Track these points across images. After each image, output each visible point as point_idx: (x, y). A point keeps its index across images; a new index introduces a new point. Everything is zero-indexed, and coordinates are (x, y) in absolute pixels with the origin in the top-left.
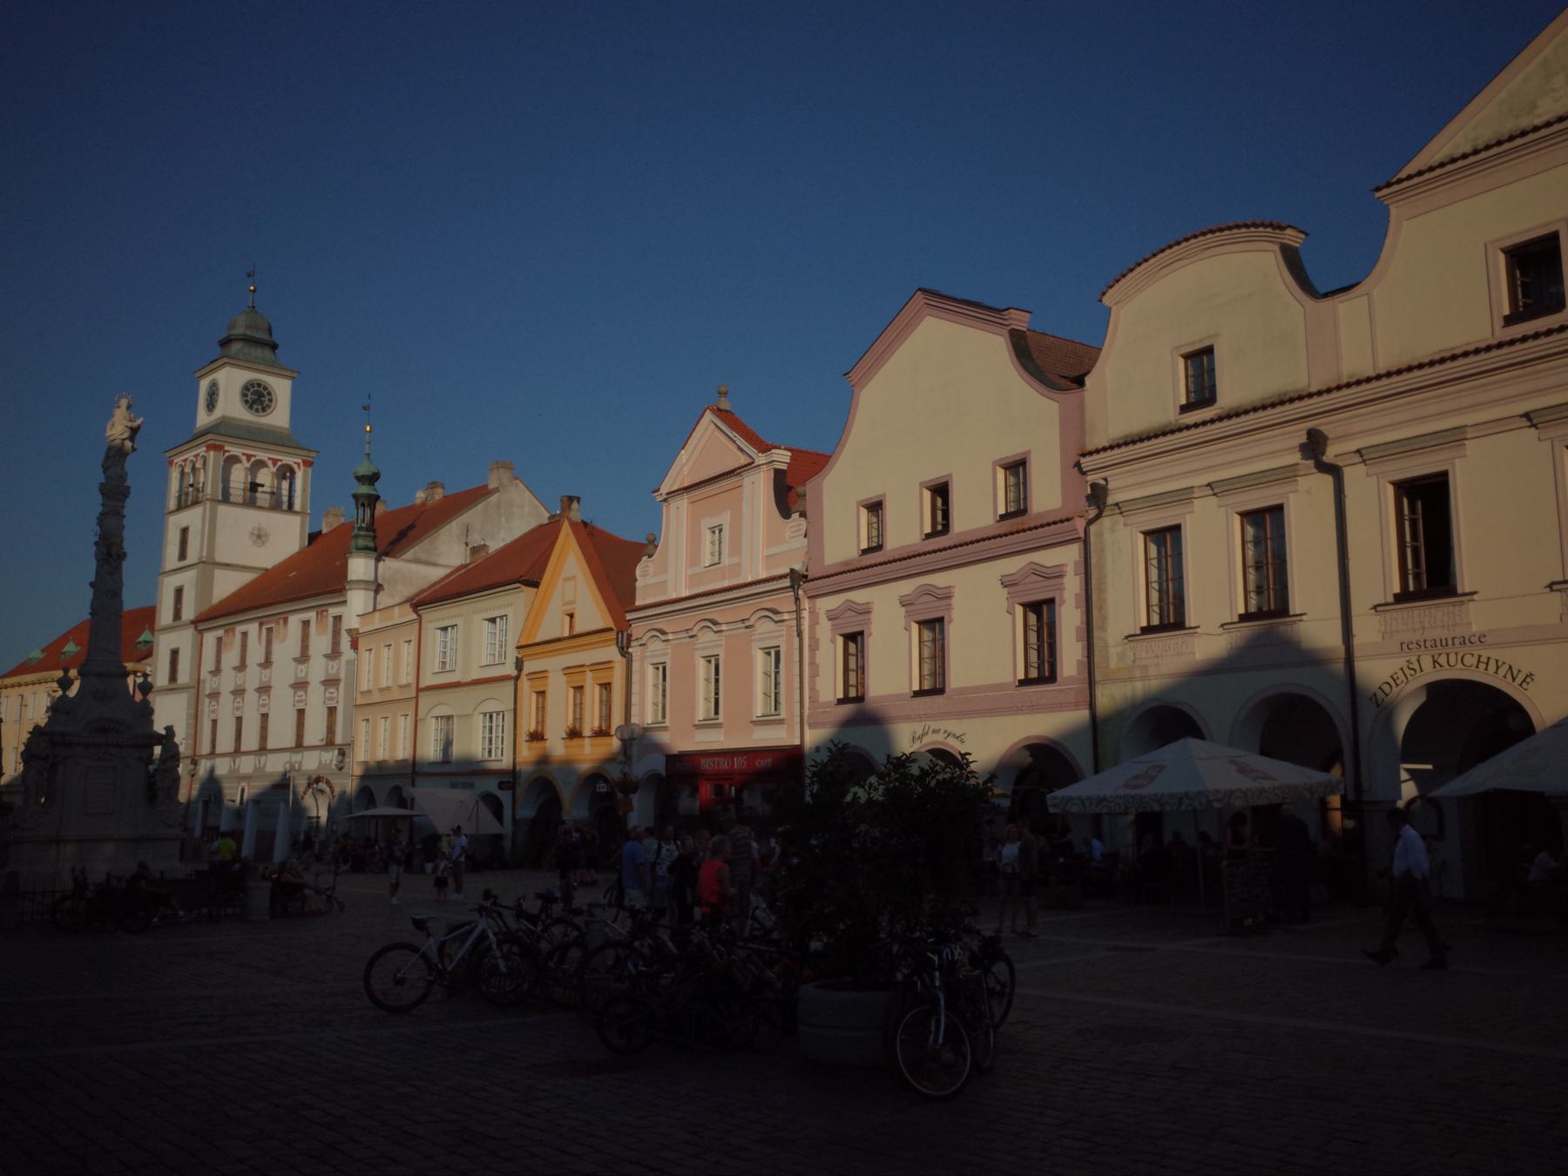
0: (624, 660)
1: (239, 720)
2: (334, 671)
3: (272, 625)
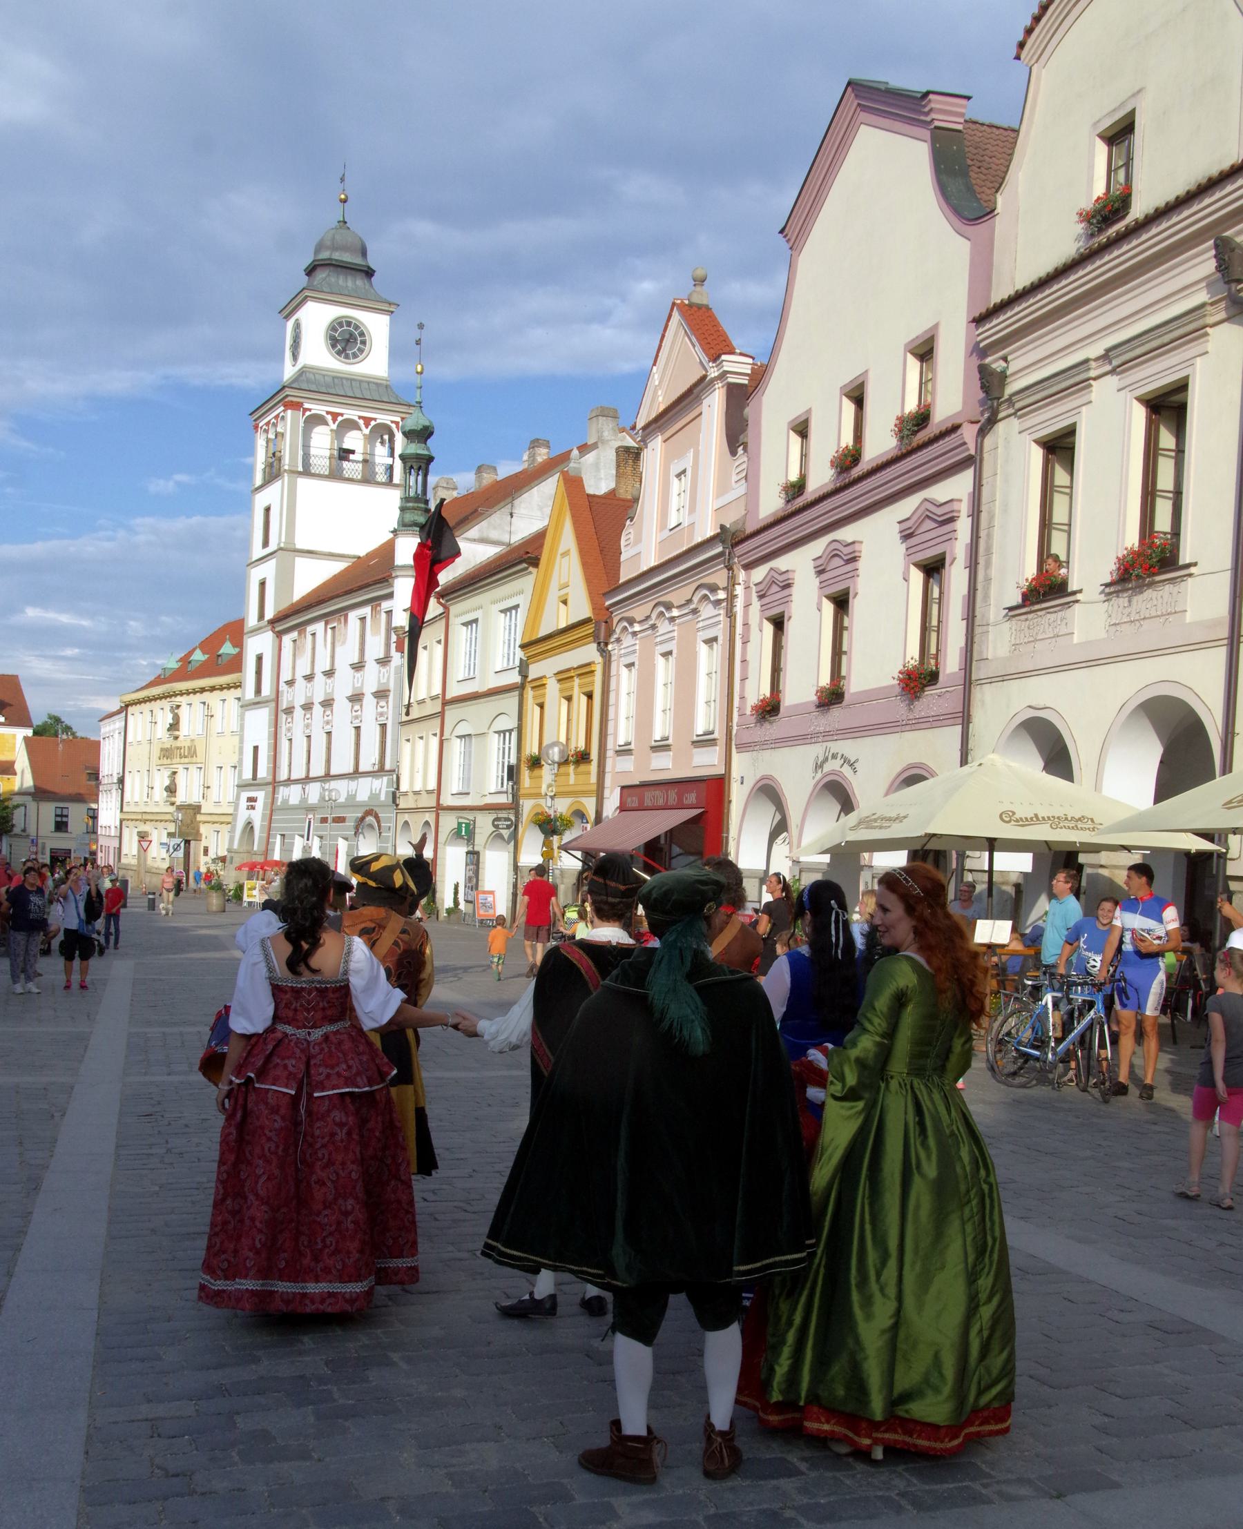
3: (335, 624)
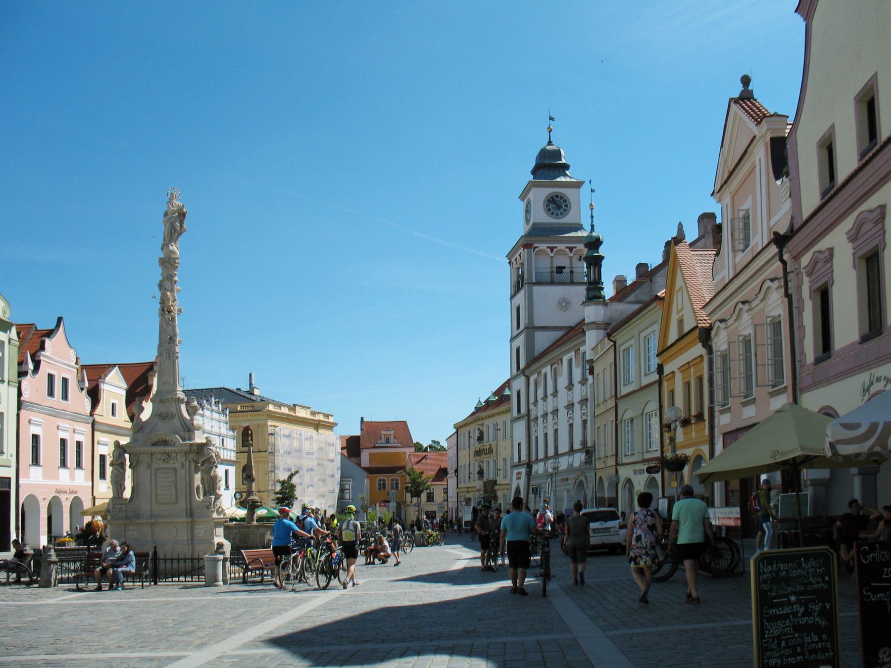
1: (546, 434)
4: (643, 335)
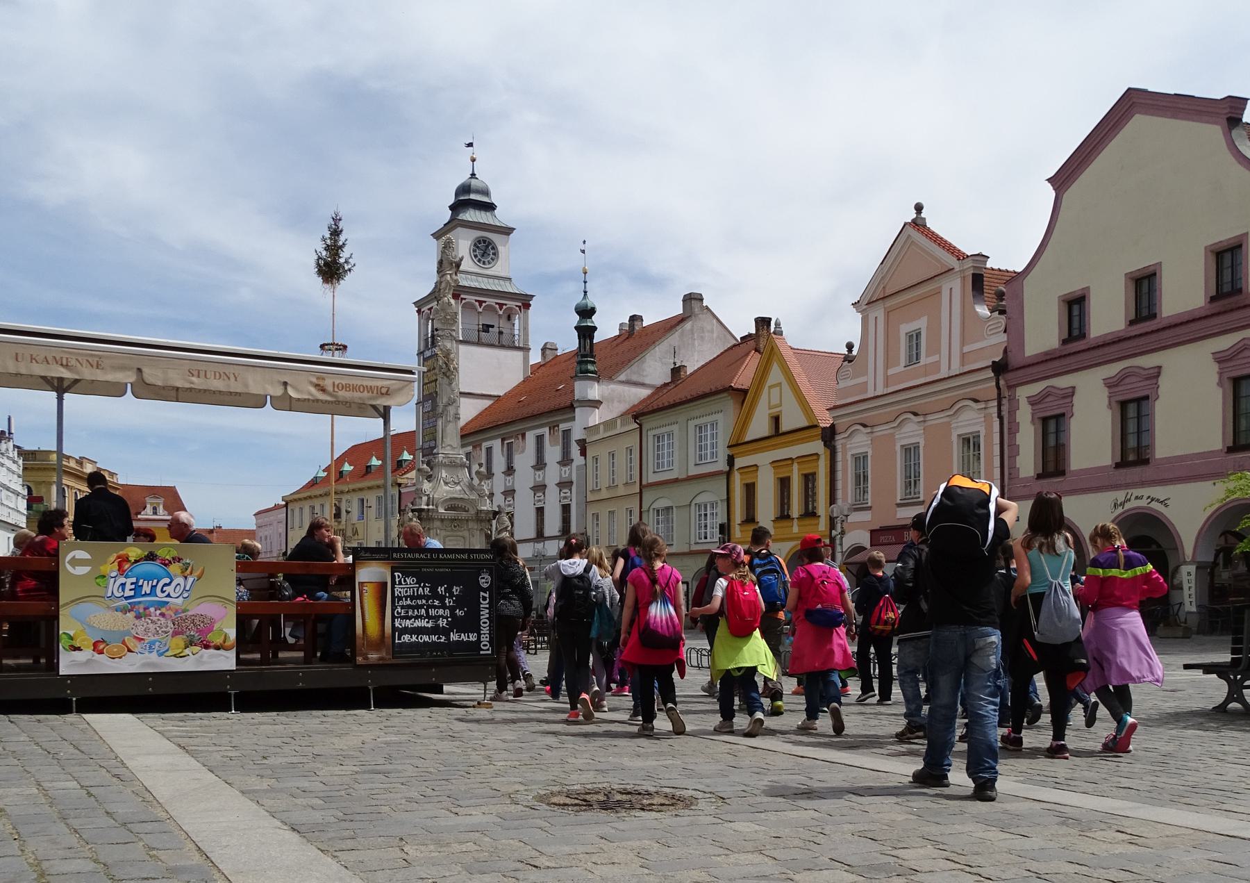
0: (828, 452)
2: (567, 475)
3: (513, 440)
4: (692, 424)
